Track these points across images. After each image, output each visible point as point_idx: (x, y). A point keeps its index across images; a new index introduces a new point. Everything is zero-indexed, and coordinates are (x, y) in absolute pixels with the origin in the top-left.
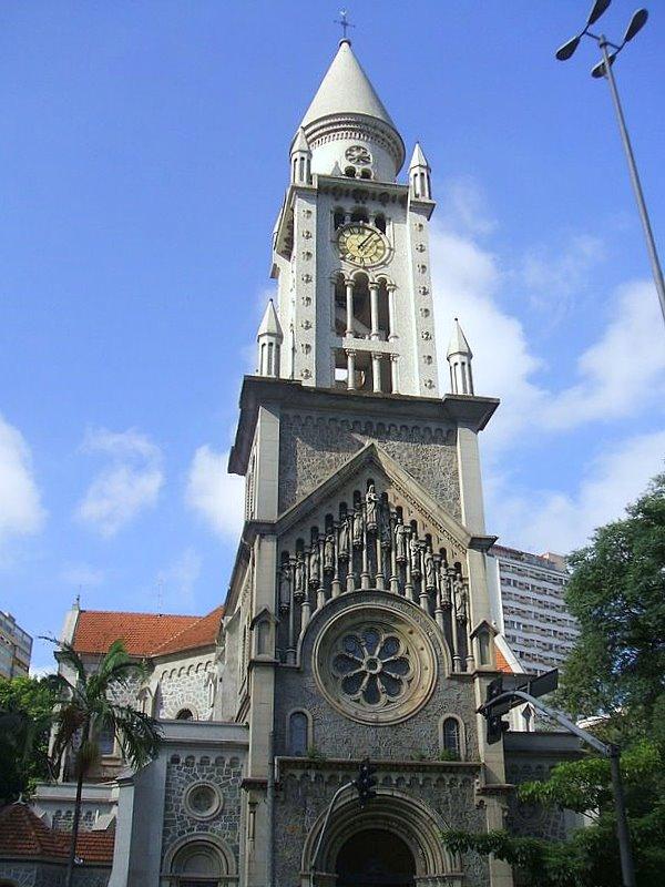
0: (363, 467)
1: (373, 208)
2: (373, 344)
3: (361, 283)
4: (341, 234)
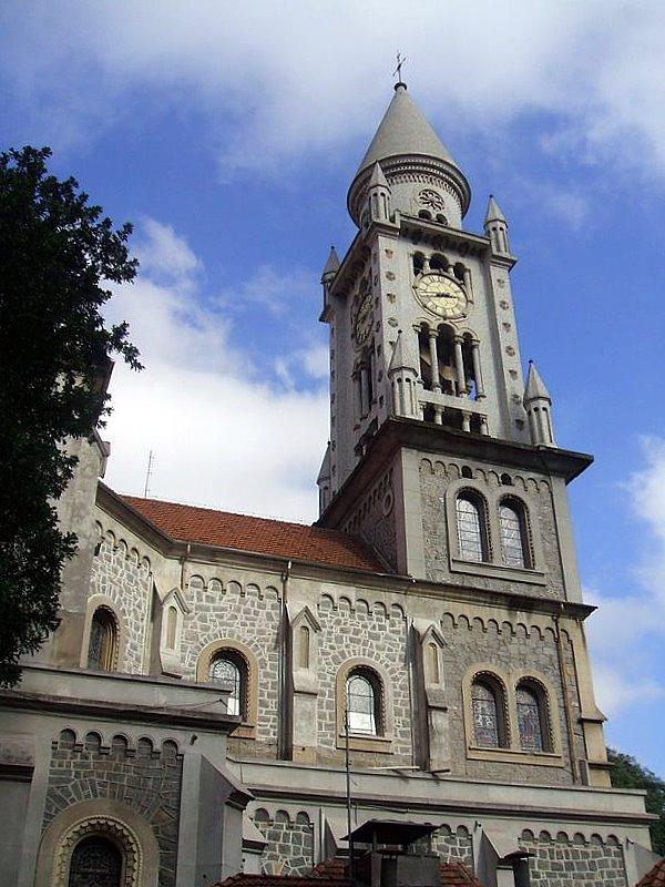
1: (452, 259)
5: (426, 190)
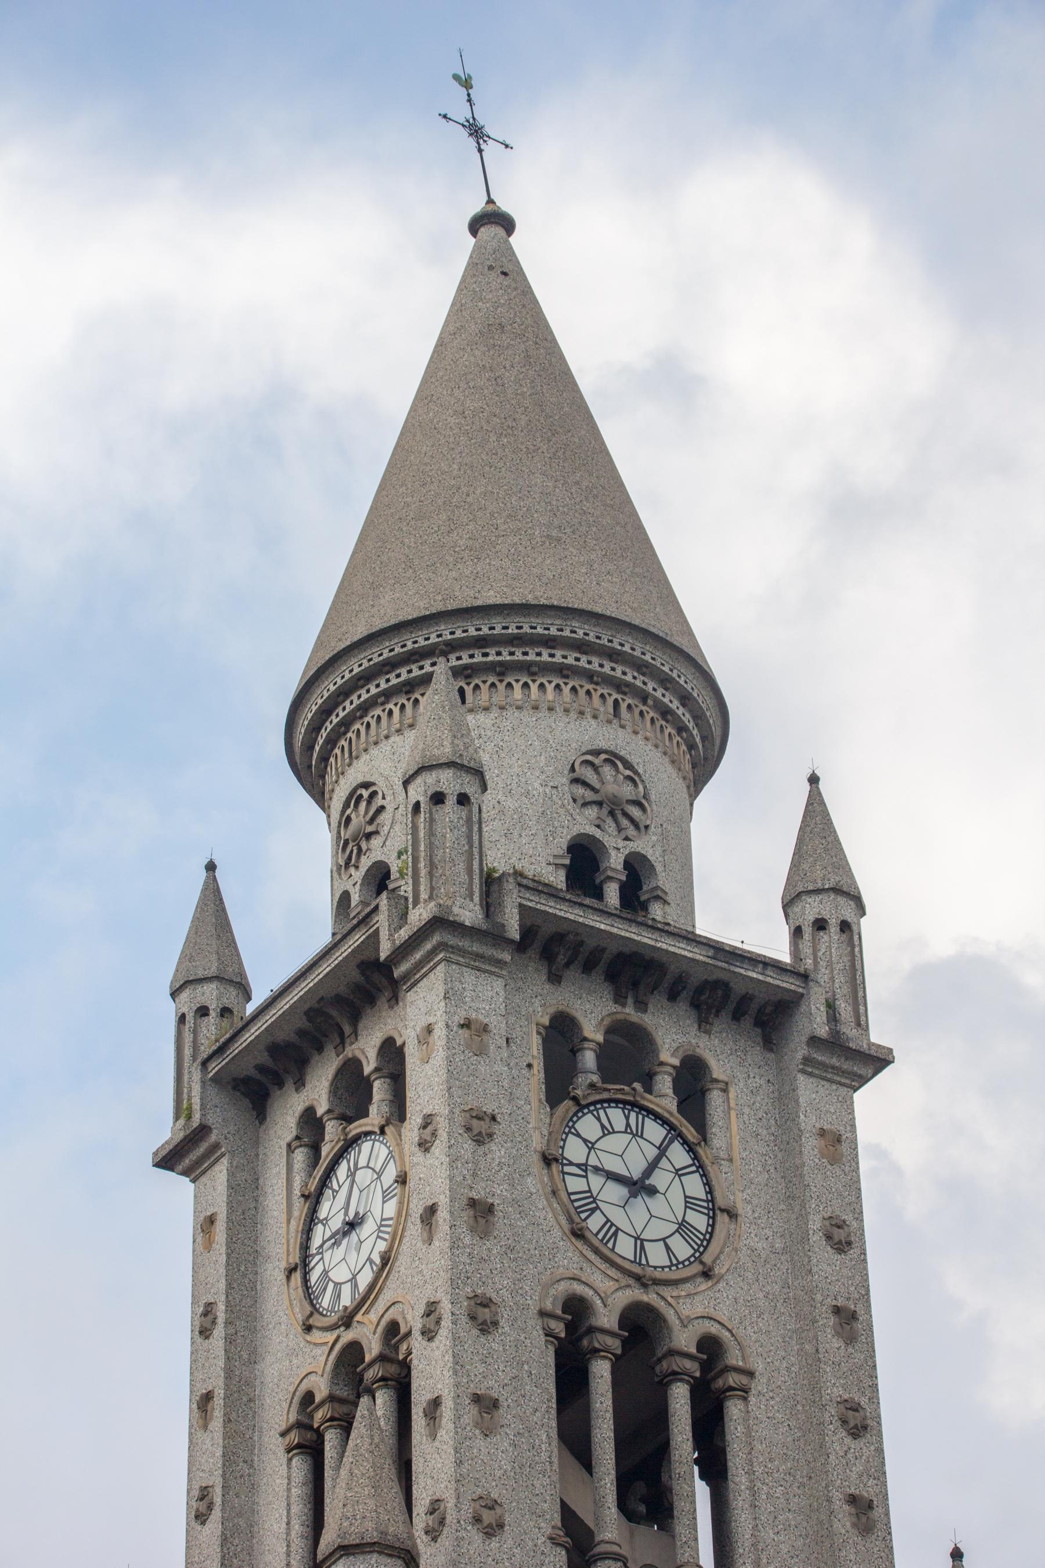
1: (672, 1035)
3: (641, 1327)
4: (570, 1128)
5: (597, 753)
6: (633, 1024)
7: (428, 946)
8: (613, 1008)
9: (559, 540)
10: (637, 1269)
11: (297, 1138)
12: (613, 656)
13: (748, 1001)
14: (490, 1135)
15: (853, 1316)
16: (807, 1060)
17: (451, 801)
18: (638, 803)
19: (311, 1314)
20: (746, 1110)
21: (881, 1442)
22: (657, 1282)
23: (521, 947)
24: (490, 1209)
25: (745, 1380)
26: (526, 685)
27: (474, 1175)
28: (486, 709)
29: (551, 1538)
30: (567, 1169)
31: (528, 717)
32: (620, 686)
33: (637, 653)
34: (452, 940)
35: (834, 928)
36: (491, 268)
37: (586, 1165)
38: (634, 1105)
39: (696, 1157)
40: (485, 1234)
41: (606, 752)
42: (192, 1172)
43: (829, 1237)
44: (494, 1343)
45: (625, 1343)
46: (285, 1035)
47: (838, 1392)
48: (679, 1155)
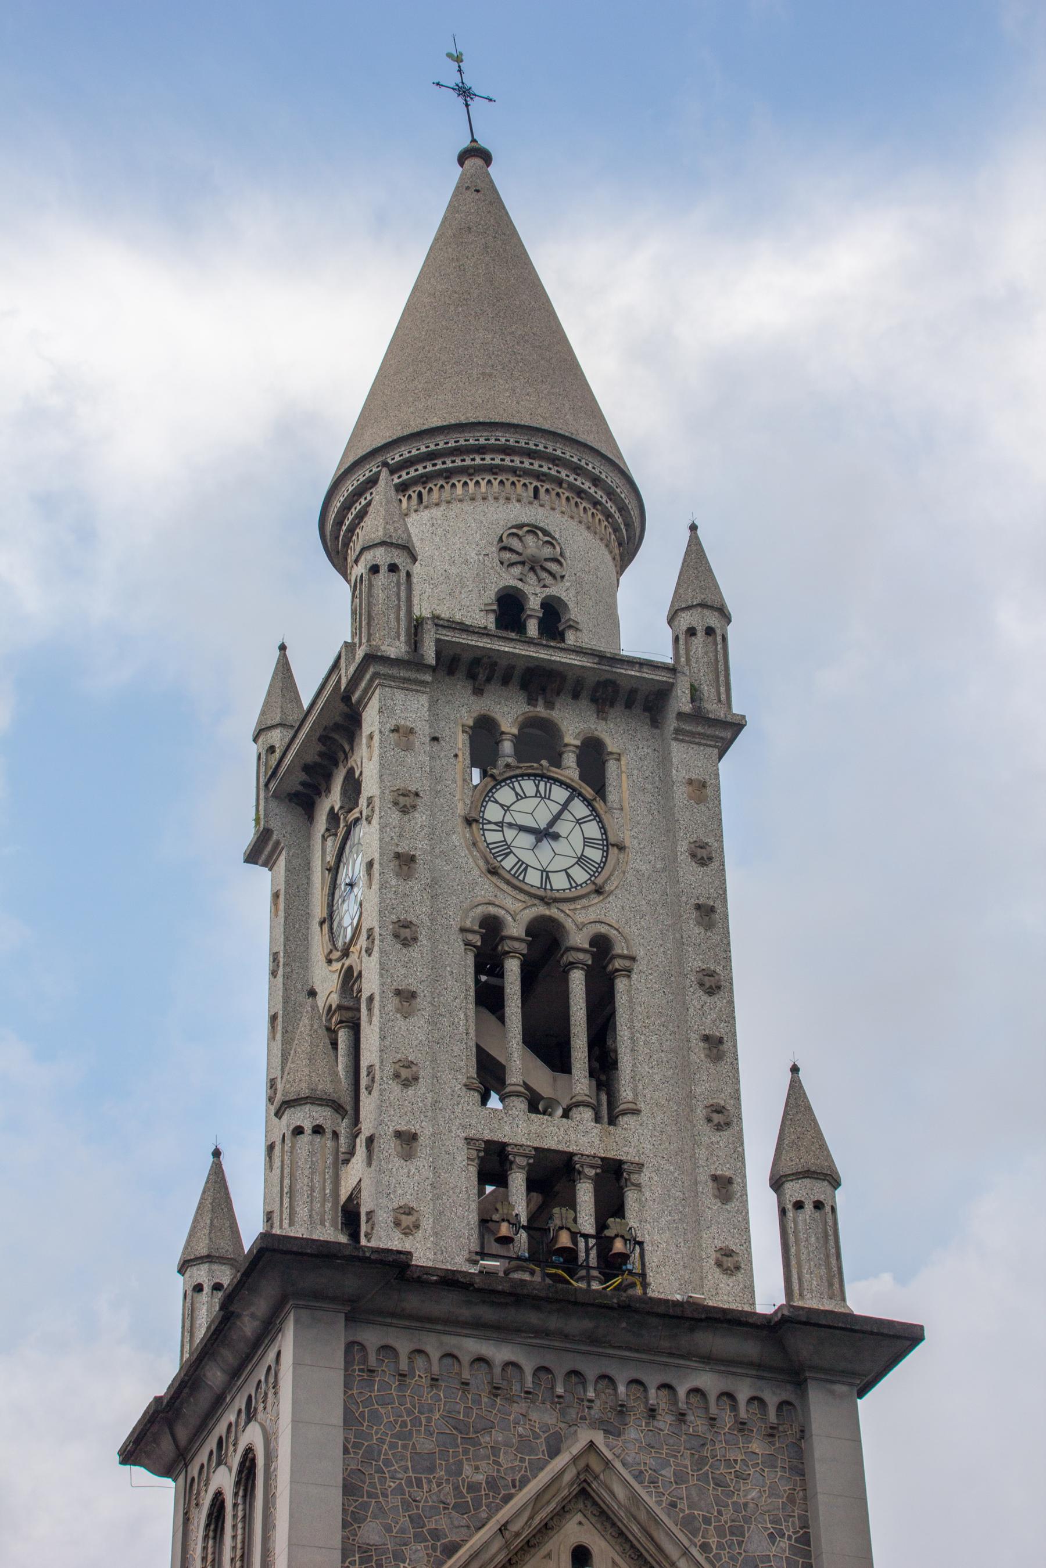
0: (562, 1512)
1: (573, 724)
2: (581, 1136)
4: (487, 795)
5: (520, 527)
6: (543, 719)
7: (368, 676)
8: (527, 708)
9: (490, 375)
10: (541, 893)
11: (327, 830)
12: (531, 454)
13: (636, 694)
14: (414, 807)
15: (713, 909)
16: (677, 731)
17: (383, 569)
18: (555, 560)
19: (331, 951)
20: (635, 772)
21: (732, 997)
22: (556, 900)
23: (434, 669)
24: (412, 859)
25: (627, 963)
26: (466, 484)
27: (400, 836)
28: (437, 505)
29: (465, 1085)
30: (486, 827)
31: (467, 506)
32: (539, 476)
33: (550, 450)
34: (383, 670)
35: (700, 633)
36: (468, 188)
37: (502, 822)
38: (543, 776)
39: (594, 809)
40: (408, 877)
41: (528, 525)
42: (269, 864)
43: (693, 856)
44: (414, 952)
45: (530, 945)
46: (311, 757)
47: (698, 964)
48: (579, 809)
